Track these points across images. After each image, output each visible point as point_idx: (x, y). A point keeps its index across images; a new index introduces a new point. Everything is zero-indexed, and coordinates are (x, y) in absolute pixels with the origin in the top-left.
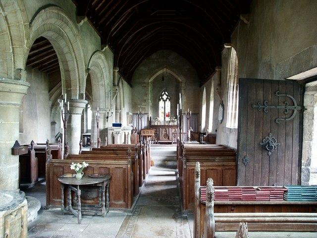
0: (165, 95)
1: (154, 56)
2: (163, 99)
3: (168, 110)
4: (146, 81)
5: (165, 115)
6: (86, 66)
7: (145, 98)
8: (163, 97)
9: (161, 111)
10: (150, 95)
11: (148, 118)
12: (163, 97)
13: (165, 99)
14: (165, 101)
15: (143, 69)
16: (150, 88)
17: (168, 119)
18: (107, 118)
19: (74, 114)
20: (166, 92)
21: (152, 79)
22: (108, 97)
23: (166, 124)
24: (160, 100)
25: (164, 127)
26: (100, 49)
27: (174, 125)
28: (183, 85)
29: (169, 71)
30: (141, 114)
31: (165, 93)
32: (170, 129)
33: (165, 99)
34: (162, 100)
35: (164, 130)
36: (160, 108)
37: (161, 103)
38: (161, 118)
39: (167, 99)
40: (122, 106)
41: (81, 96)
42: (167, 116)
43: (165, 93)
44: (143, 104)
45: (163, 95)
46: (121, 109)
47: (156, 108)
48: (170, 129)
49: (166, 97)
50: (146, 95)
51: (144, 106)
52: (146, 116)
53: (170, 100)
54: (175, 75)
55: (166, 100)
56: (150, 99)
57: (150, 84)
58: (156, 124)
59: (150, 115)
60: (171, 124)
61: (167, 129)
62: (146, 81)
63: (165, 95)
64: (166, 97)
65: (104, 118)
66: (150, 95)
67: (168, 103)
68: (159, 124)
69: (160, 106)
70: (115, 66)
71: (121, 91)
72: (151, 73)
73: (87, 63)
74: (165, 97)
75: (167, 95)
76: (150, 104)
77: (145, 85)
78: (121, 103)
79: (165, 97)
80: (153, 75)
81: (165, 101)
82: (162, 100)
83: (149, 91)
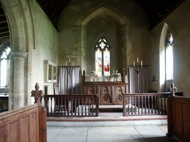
0: (102, 43)
2: (100, 48)
3: (107, 62)
4: (77, 23)
5: (104, 69)
7: (76, 45)
8: (100, 45)
9: (98, 63)
10: (83, 42)
11: (80, 72)
12: (100, 45)
13: (103, 48)
14: (102, 51)
15: (73, 8)
16: (82, 32)
17: (107, 74)
20: (104, 40)
21: (84, 23)
23: (106, 81)
24: (96, 49)
25: (104, 84)
27: (116, 82)
28: (127, 28)
30: (70, 67)
31: (102, 41)
32: (113, 87)
33: (103, 48)
34: (98, 50)
35: (104, 88)
36: (96, 59)
37: (98, 54)
38: (98, 72)
39: (105, 47)
40: (31, 46)
42: (106, 70)
43: (102, 41)
44: (74, 53)
45: (100, 43)
46: (27, 51)
47: (91, 60)
48: (113, 87)
49: (105, 45)
50: (78, 41)
51: (75, 57)
52: (78, 70)
53: (109, 49)
54: (115, 16)
55: (104, 49)
56: (82, 46)
57: (82, 27)
58: (92, 80)
59: (83, 68)
60: (112, 80)
61: (109, 88)
62: (77, 23)
63: (102, 43)
64: (105, 45)
66: (83, 42)
67: (107, 54)
68: (96, 81)
71: (27, 14)
72: (85, 14)
74: (102, 45)
75: (105, 43)
76: (84, 54)
78: (27, 39)
79: (102, 45)
80: (87, 15)
81: (102, 51)
82: (98, 50)
83: (82, 35)
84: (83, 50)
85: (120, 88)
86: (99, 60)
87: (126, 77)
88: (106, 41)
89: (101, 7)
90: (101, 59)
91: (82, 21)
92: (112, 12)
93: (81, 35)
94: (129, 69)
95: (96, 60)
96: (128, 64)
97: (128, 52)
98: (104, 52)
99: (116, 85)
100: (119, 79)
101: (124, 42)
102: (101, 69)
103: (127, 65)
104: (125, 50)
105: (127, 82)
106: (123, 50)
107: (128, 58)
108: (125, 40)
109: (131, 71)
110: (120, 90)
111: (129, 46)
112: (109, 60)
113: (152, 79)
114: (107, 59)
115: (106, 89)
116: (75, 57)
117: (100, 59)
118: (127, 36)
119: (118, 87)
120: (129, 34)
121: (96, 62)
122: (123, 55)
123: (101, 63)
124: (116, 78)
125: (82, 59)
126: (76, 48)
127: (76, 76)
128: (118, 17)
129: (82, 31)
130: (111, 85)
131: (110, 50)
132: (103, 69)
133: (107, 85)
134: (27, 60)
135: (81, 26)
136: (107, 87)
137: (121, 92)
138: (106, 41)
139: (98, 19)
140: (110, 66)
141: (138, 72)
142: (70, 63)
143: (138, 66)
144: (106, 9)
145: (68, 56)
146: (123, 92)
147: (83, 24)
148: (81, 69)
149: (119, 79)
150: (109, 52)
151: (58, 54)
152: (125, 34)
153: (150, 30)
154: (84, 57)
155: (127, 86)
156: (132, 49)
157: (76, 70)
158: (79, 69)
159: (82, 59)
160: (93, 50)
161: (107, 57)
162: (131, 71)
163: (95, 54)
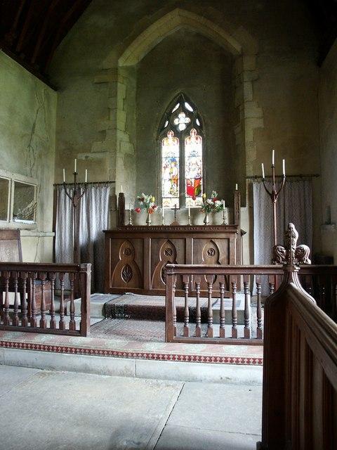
0: (182, 115)
2: (174, 128)
3: (194, 169)
4: (106, 64)
8: (176, 121)
9: (168, 173)
10: (121, 117)
11: (113, 198)
13: (182, 127)
14: (181, 136)
15: (96, 22)
20: (187, 106)
21: (129, 59)
23: (183, 223)
24: (163, 133)
27: (214, 226)
28: (248, 63)
31: (183, 109)
32: (191, 242)
33: (182, 127)
34: (170, 134)
37: (169, 147)
39: (189, 126)
42: (191, 192)
43: (183, 109)
44: (97, 145)
45: (176, 115)
47: (147, 164)
48: (191, 242)
49: (188, 120)
50: (108, 111)
51: (99, 156)
55: (187, 132)
56: (121, 124)
57: (121, 72)
58: (142, 222)
60: (200, 222)
62: (106, 64)
63: (182, 115)
64: (188, 120)
67: (195, 145)
69: (164, 155)
72: (126, 36)
74: (182, 121)
75: (188, 114)
79: (182, 121)
81: (181, 136)
82: (170, 134)
84: (122, 136)
85: (212, 246)
86: (173, 164)
87: (244, 212)
88: (191, 109)
89: (170, 9)
90: (178, 160)
91: (120, 54)
92: (202, 20)
93: (116, 96)
94: (251, 186)
95: (163, 165)
96: (250, 171)
97: (249, 136)
98: (187, 140)
99: (201, 235)
100: (223, 218)
101: (241, 108)
102: (176, 188)
103: (248, 174)
104: (243, 130)
105: (244, 226)
106: (238, 130)
107: (251, 154)
108: (243, 102)
109: (258, 194)
110: (212, 250)
111: (253, 119)
112: (200, 164)
113: (325, 219)
114: (193, 160)
115: (169, 246)
116: (99, 156)
117: (173, 160)
118: (247, 89)
119: (205, 241)
120: (253, 82)
121: (163, 169)
122: (237, 146)
123: (176, 171)
124: (214, 213)
125: (120, 163)
126: (104, 132)
127: (100, 210)
128: (222, 33)
129: (119, 84)
130: (185, 236)
131: (201, 135)
132: (182, 190)
133: (173, 236)
135: (115, 71)
136: (173, 242)
137: (214, 258)
138: (191, 109)
140: (202, 181)
141: (272, 196)
142: (75, 174)
143: (273, 176)
144: (186, 13)
146: (223, 257)
147: (121, 63)
148: (114, 190)
149: (223, 218)
150: (200, 141)
151: (57, 150)
152: (241, 83)
153: (319, 63)
154: (127, 156)
155: (246, 238)
156: (263, 127)
157: (100, 192)
158: (108, 190)
159: (120, 163)
160: (155, 135)
161: (194, 156)
162: (258, 194)
163: (159, 146)
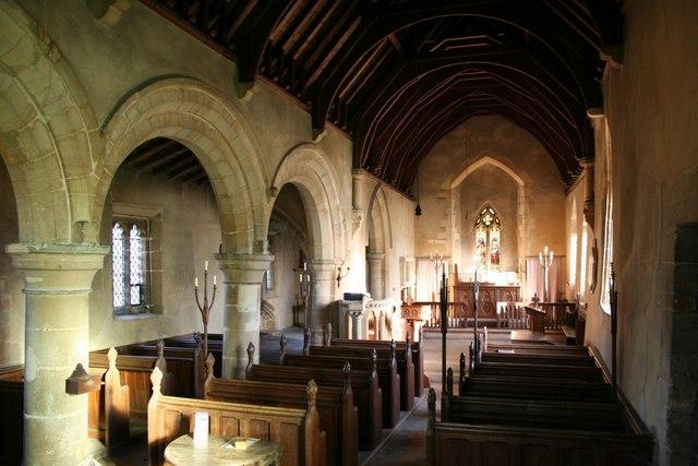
1: (460, 132)
2: (484, 223)
4: (443, 186)
6: (266, 181)
7: (444, 223)
10: (453, 217)
15: (436, 160)
16: (453, 201)
18: (339, 279)
19: (249, 284)
21: (458, 182)
22: (340, 235)
26: (309, 139)
29: (495, 163)
34: (481, 226)
39: (492, 222)
40: (387, 245)
41: (258, 247)
44: (440, 235)
46: (384, 252)
50: (446, 215)
51: (441, 242)
54: (508, 170)
56: (453, 225)
57: (453, 192)
62: (443, 186)
65: (333, 279)
70: (355, 167)
71: (384, 213)
73: (270, 177)
74: (488, 219)
75: (492, 215)
77: (440, 195)
80: (460, 172)
82: (481, 226)
89: (483, 156)
91: (452, 181)
134: (384, 262)
135: (450, 191)
139: (482, 172)
145: (431, 242)
147: (453, 186)
